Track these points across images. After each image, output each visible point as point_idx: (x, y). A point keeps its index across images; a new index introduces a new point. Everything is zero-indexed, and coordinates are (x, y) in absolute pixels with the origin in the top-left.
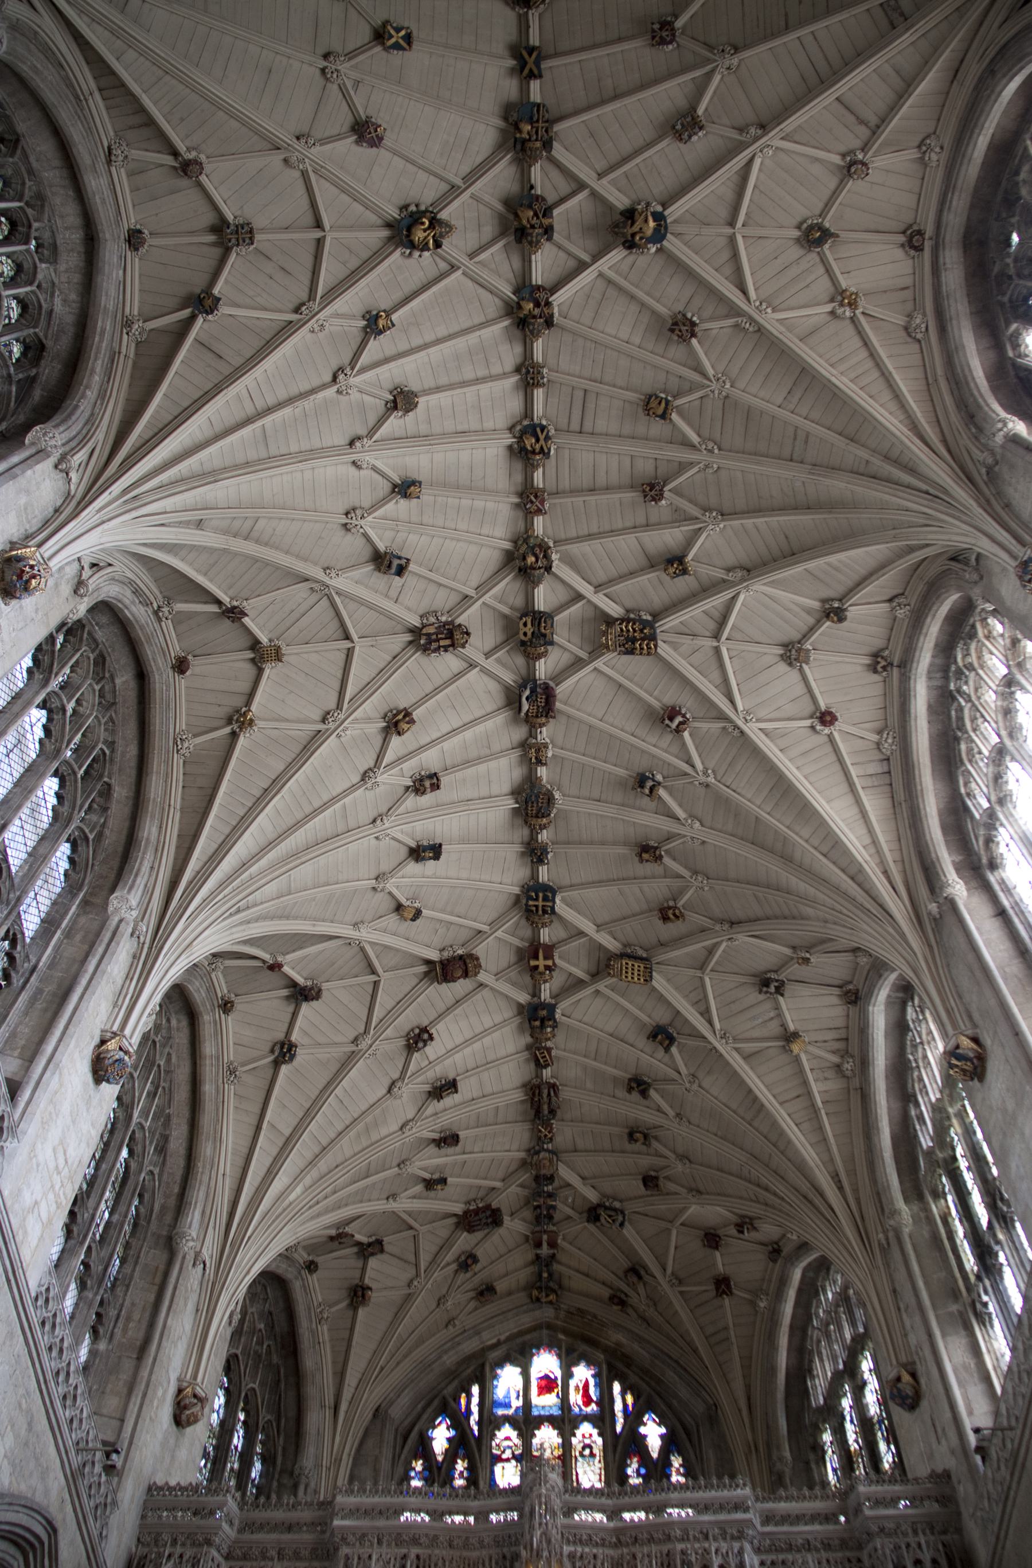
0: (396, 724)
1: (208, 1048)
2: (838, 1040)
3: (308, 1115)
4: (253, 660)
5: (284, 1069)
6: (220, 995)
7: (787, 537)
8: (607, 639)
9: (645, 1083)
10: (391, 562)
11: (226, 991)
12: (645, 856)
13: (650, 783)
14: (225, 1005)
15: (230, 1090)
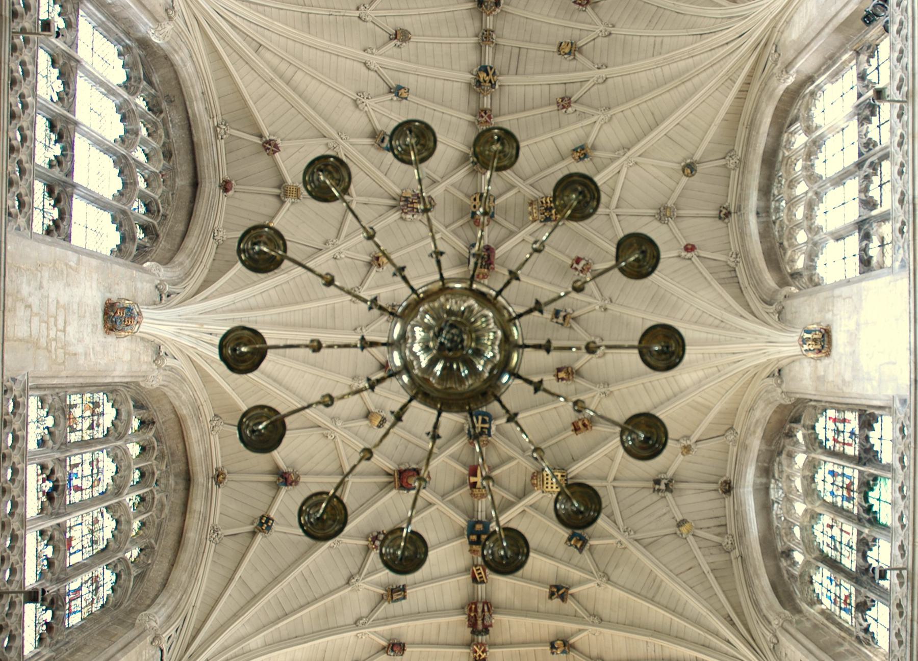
0: (378, 258)
1: (197, 505)
2: (719, 526)
3: (276, 580)
4: (278, 196)
5: (260, 537)
6: (215, 466)
7: (653, 114)
8: (532, 209)
9: (563, 587)
10: (384, 138)
11: (220, 465)
12: (561, 375)
13: (562, 314)
14: (218, 476)
15: (211, 548)
